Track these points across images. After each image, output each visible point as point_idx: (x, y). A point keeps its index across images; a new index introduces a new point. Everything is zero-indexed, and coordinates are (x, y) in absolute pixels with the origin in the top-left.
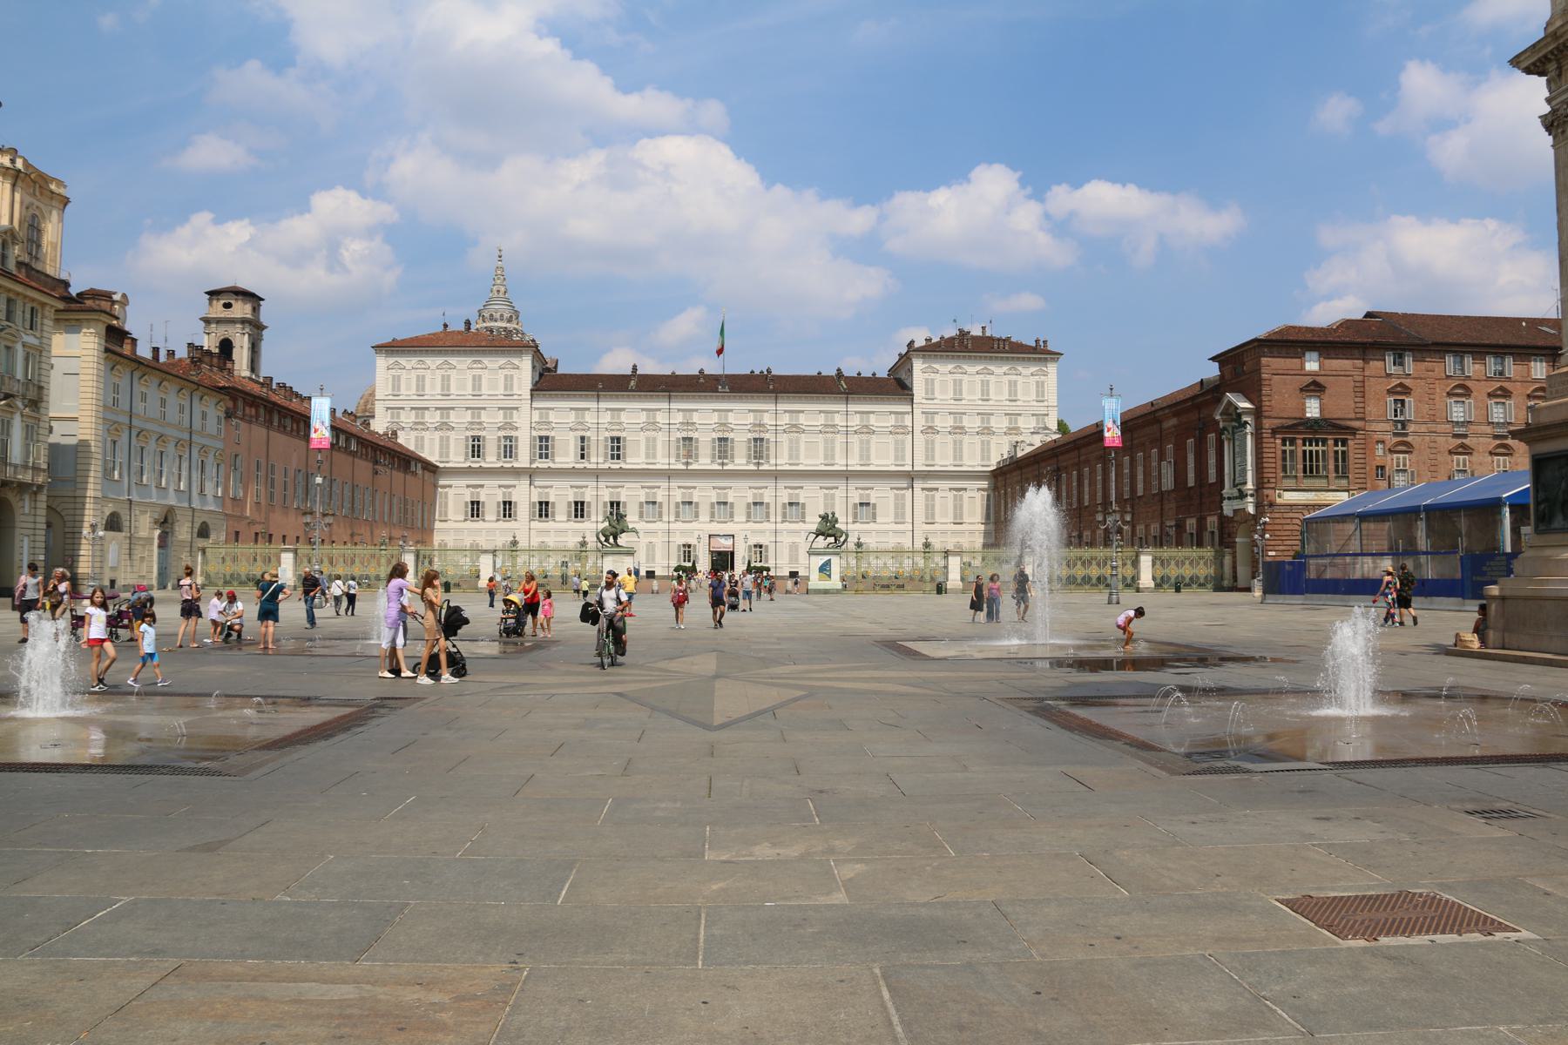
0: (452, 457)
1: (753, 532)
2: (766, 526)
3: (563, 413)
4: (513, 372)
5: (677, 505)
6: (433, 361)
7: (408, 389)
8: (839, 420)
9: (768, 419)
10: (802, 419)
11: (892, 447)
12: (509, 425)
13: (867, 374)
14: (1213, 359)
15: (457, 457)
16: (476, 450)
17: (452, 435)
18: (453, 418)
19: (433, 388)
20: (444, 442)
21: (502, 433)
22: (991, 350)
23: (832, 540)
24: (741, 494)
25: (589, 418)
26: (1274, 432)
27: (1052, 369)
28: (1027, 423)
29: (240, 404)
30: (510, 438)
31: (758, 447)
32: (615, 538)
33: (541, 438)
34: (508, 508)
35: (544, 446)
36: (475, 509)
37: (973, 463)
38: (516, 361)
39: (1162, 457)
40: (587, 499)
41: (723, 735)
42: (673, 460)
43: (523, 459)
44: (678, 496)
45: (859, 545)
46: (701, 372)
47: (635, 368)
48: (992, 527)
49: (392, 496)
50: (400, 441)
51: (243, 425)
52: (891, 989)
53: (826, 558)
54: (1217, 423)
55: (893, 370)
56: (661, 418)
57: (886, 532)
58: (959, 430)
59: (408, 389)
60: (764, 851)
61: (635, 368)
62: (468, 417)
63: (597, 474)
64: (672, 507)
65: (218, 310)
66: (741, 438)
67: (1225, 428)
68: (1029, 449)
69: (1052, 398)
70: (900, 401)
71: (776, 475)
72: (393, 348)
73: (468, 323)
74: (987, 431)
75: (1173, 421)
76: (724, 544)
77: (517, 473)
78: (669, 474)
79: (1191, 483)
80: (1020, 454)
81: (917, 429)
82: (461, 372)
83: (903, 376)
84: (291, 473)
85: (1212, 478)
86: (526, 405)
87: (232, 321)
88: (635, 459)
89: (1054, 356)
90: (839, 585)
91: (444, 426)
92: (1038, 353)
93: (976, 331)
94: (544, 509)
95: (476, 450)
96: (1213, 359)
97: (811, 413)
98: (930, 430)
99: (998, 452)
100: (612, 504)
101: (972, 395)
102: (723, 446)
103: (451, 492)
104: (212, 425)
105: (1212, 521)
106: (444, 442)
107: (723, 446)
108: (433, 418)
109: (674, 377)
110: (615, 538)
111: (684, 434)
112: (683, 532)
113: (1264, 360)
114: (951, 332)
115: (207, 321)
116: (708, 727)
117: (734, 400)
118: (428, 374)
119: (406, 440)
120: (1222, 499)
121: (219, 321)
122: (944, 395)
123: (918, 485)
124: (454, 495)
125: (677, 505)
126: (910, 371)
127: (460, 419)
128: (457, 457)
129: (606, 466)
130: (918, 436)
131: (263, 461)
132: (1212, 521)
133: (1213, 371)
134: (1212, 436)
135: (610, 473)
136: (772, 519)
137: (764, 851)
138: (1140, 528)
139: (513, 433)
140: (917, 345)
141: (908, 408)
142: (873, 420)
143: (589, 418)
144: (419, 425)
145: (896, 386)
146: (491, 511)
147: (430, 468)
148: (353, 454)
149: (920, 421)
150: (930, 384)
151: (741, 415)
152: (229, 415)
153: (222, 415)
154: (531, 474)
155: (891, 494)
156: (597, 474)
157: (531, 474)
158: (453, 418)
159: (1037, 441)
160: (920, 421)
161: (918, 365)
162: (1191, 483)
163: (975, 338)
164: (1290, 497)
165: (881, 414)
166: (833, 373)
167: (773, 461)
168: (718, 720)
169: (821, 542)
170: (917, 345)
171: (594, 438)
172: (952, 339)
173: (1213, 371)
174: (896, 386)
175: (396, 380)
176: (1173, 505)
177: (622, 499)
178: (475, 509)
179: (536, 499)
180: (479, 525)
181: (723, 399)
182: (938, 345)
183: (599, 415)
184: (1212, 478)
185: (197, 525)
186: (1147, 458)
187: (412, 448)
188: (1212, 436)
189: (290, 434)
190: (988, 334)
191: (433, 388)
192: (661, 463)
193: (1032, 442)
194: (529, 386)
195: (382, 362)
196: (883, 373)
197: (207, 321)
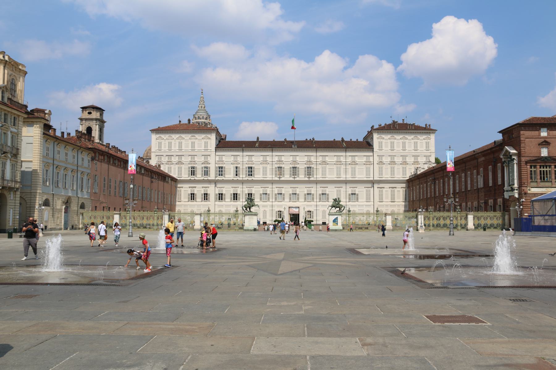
0: (183, 175)
1: (307, 206)
2: (312, 203)
3: (229, 158)
4: (208, 140)
5: (276, 194)
6: (175, 136)
7: (165, 147)
8: (342, 159)
9: (313, 159)
10: (327, 159)
11: (365, 170)
12: (206, 162)
13: (354, 140)
14: (500, 132)
15: (185, 176)
16: (193, 173)
17: (183, 166)
18: (183, 159)
19: (175, 147)
20: (180, 170)
21: (203, 166)
22: (406, 129)
23: (338, 209)
24: (302, 190)
25: (239, 159)
26: (527, 163)
27: (432, 136)
28: (422, 160)
29: (97, 154)
30: (207, 168)
31: (309, 171)
32: (250, 209)
33: (219, 167)
34: (206, 196)
35: (221, 171)
36: (193, 197)
37: (399, 176)
38: (209, 136)
39: (478, 174)
40: (238, 192)
41: (281, 276)
42: (274, 176)
43: (212, 176)
44: (276, 191)
45: (349, 211)
46: (285, 139)
47: (258, 138)
48: (407, 203)
49: (158, 191)
50: (161, 169)
51: (99, 163)
52: (307, 328)
53: (336, 217)
54: (501, 159)
55: (365, 138)
56: (269, 159)
57: (363, 205)
58: (393, 163)
59: (165, 147)
60: (285, 303)
61: (258, 138)
62: (189, 159)
63: (243, 182)
64: (274, 195)
65: (86, 115)
66: (302, 167)
67: (505, 161)
68: (422, 171)
69: (432, 148)
70: (368, 151)
71: (317, 182)
72: (158, 131)
73: (189, 120)
74: (405, 163)
75: (483, 159)
76: (295, 211)
77: (210, 182)
78: (272, 182)
79: (491, 184)
80: (419, 173)
81: (375, 162)
82: (186, 141)
83: (369, 141)
84: (118, 183)
85: (500, 183)
86: (213, 154)
87: (92, 119)
88: (258, 176)
89: (433, 131)
90: (341, 228)
91: (180, 163)
92: (427, 130)
93: (400, 122)
94: (221, 197)
95: (193, 173)
96: (500, 132)
97: (331, 156)
98: (381, 163)
99: (409, 172)
100: (249, 194)
101: (398, 148)
102: (294, 170)
103: (182, 189)
104: (86, 163)
105: (500, 201)
106: (180, 170)
107: (294, 170)
108: (175, 159)
109: (274, 142)
110: (250, 209)
111: (278, 166)
112: (278, 206)
113: (522, 132)
114: (389, 122)
115: (81, 119)
116: (276, 275)
117: (299, 151)
118: (173, 141)
119: (164, 169)
120: (504, 191)
121: (86, 120)
122: (386, 148)
123: (376, 186)
124: (184, 191)
125: (276, 194)
126: (372, 138)
128: (185, 176)
129: (246, 179)
130: (376, 166)
131: (106, 178)
132: (500, 201)
133: (500, 137)
134: (499, 165)
135: (248, 181)
136: (315, 200)
137: (285, 303)
138: (469, 204)
139: (208, 166)
140: (375, 127)
141: (371, 154)
142: (357, 159)
143: (239, 159)
144: (169, 162)
145: (366, 145)
146: (199, 197)
147: (174, 180)
148: (143, 174)
150: (380, 144)
151: (302, 158)
152: (93, 159)
153: (90, 159)
154: (215, 182)
155: (365, 190)
156: (243, 182)
157: (215, 182)
158: (183, 159)
159: (426, 167)
160: (376, 159)
161: (375, 136)
162: (491, 184)
163: (399, 124)
164: (534, 190)
165: (360, 156)
166: (340, 139)
167: (315, 176)
168: (279, 273)
169: (334, 210)
170: (375, 127)
171: (241, 167)
172: (390, 125)
173: (500, 137)
174: (366, 145)
175: (160, 144)
176: (483, 194)
177: (253, 192)
178: (193, 197)
179: (217, 192)
180: (194, 203)
181: (294, 151)
182: (384, 127)
183: (243, 158)
184: (500, 183)
185: (80, 204)
186: (472, 174)
187: (166, 172)
188: (499, 165)
189: (117, 166)
190: (405, 122)
191: (175, 147)
192: (269, 177)
193: (424, 168)
194: (214, 146)
195: (154, 136)
196: (361, 139)
197: (81, 119)
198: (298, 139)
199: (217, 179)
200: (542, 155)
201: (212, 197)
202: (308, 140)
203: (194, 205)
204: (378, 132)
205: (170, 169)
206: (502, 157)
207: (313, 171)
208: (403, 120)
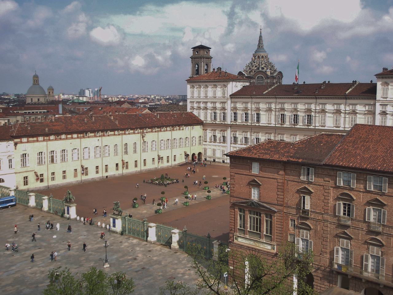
7: (196, 95)
8: (342, 107)
9: (313, 107)
12: (224, 109)
19: (202, 95)
25: (249, 105)
56: (273, 106)
59: (196, 95)
70: (370, 99)
77: (227, 126)
78: (275, 128)
86: (229, 102)
108: (202, 105)
117: (300, 98)
119: (195, 113)
127: (210, 105)
143: (249, 105)
144: (199, 108)
145: (368, 92)
149: (379, 109)
157: (231, 126)
167: (314, 125)
175: (193, 93)
180: (216, 144)
199: (232, 123)
201: (228, 140)
203: (216, 146)
204: (383, 78)
205: (199, 113)
207: (312, 119)
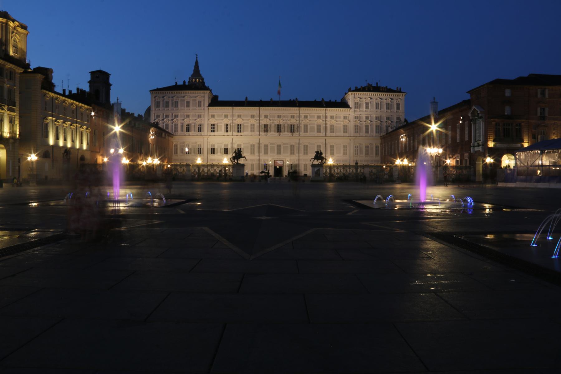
13: (333, 100)
23: (320, 161)
32: (237, 161)
47: (246, 98)
53: (318, 168)
54: (469, 117)
61: (246, 98)
79: (458, 141)
85: (467, 139)
93: (374, 85)
96: (468, 92)
110: (237, 161)
141: (349, 113)
150: (356, 105)
162: (458, 141)
172: (365, 87)
184: (467, 139)
190: (379, 86)
198: (282, 99)
200: (506, 114)
202: (292, 100)
205: (167, 125)
206: (470, 115)
208: (377, 83)
